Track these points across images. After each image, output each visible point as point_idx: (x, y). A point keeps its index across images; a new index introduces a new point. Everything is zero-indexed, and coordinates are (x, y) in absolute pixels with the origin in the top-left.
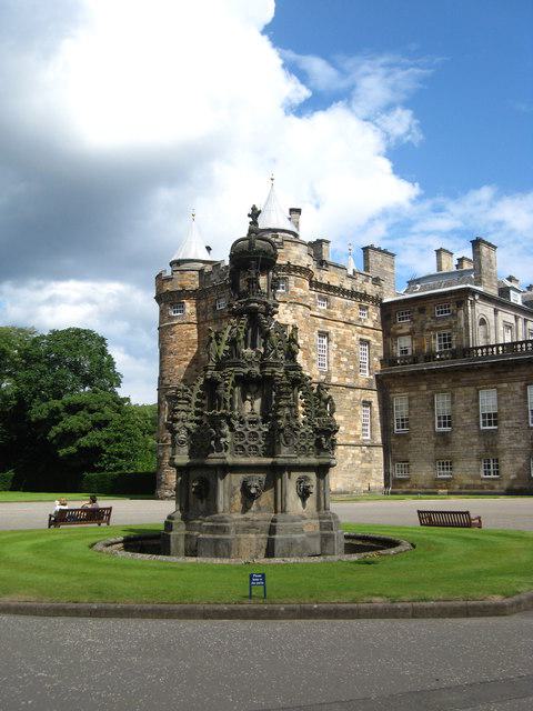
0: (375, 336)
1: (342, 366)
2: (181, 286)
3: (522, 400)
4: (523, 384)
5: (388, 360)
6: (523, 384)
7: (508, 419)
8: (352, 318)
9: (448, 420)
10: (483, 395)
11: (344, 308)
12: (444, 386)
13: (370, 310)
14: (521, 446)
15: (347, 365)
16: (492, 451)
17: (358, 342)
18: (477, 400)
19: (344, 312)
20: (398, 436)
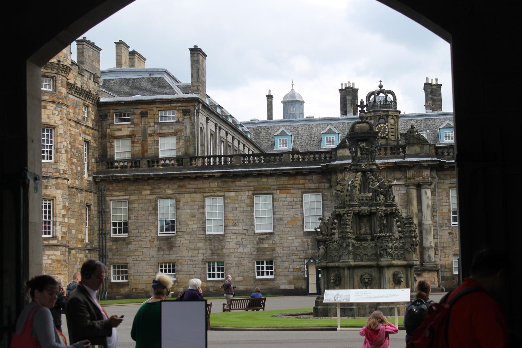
0: (93, 136)
1: (74, 167)
3: (249, 208)
4: (250, 193)
5: (105, 159)
6: (250, 193)
7: (235, 225)
8: (80, 118)
9: (172, 226)
10: (208, 202)
12: (169, 191)
13: (90, 109)
14: (246, 250)
15: (77, 167)
16: (218, 255)
17: (83, 143)
18: (203, 207)
19: (74, 113)
20: (116, 240)
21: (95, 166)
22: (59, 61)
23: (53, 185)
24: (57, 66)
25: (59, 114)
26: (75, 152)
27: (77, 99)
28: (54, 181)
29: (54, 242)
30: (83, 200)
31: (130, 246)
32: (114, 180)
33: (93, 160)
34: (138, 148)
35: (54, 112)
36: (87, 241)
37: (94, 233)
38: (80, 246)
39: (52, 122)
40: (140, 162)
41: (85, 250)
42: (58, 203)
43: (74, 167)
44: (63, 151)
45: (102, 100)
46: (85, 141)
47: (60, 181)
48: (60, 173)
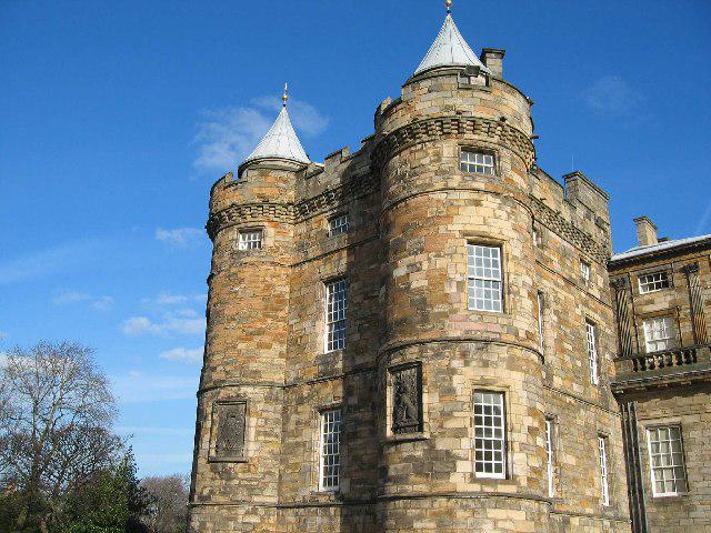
0: (603, 314)
2: (260, 196)
5: (628, 354)
8: (574, 276)
11: (564, 255)
15: (573, 359)
21: (613, 368)
22: (503, 119)
23: (503, 360)
24: (499, 128)
25: (509, 218)
26: (568, 331)
27: (566, 244)
28: (503, 352)
29: (511, 489)
30: (592, 422)
31: (692, 515)
32: (649, 388)
33: (607, 356)
34: (686, 328)
35: (498, 212)
36: (607, 504)
37: (618, 489)
38: (589, 510)
39: (494, 232)
40: (694, 353)
41: (603, 516)
42: (514, 400)
43: (567, 358)
44: (524, 292)
45: (614, 258)
46: (588, 321)
47: (518, 352)
48: (517, 335)
